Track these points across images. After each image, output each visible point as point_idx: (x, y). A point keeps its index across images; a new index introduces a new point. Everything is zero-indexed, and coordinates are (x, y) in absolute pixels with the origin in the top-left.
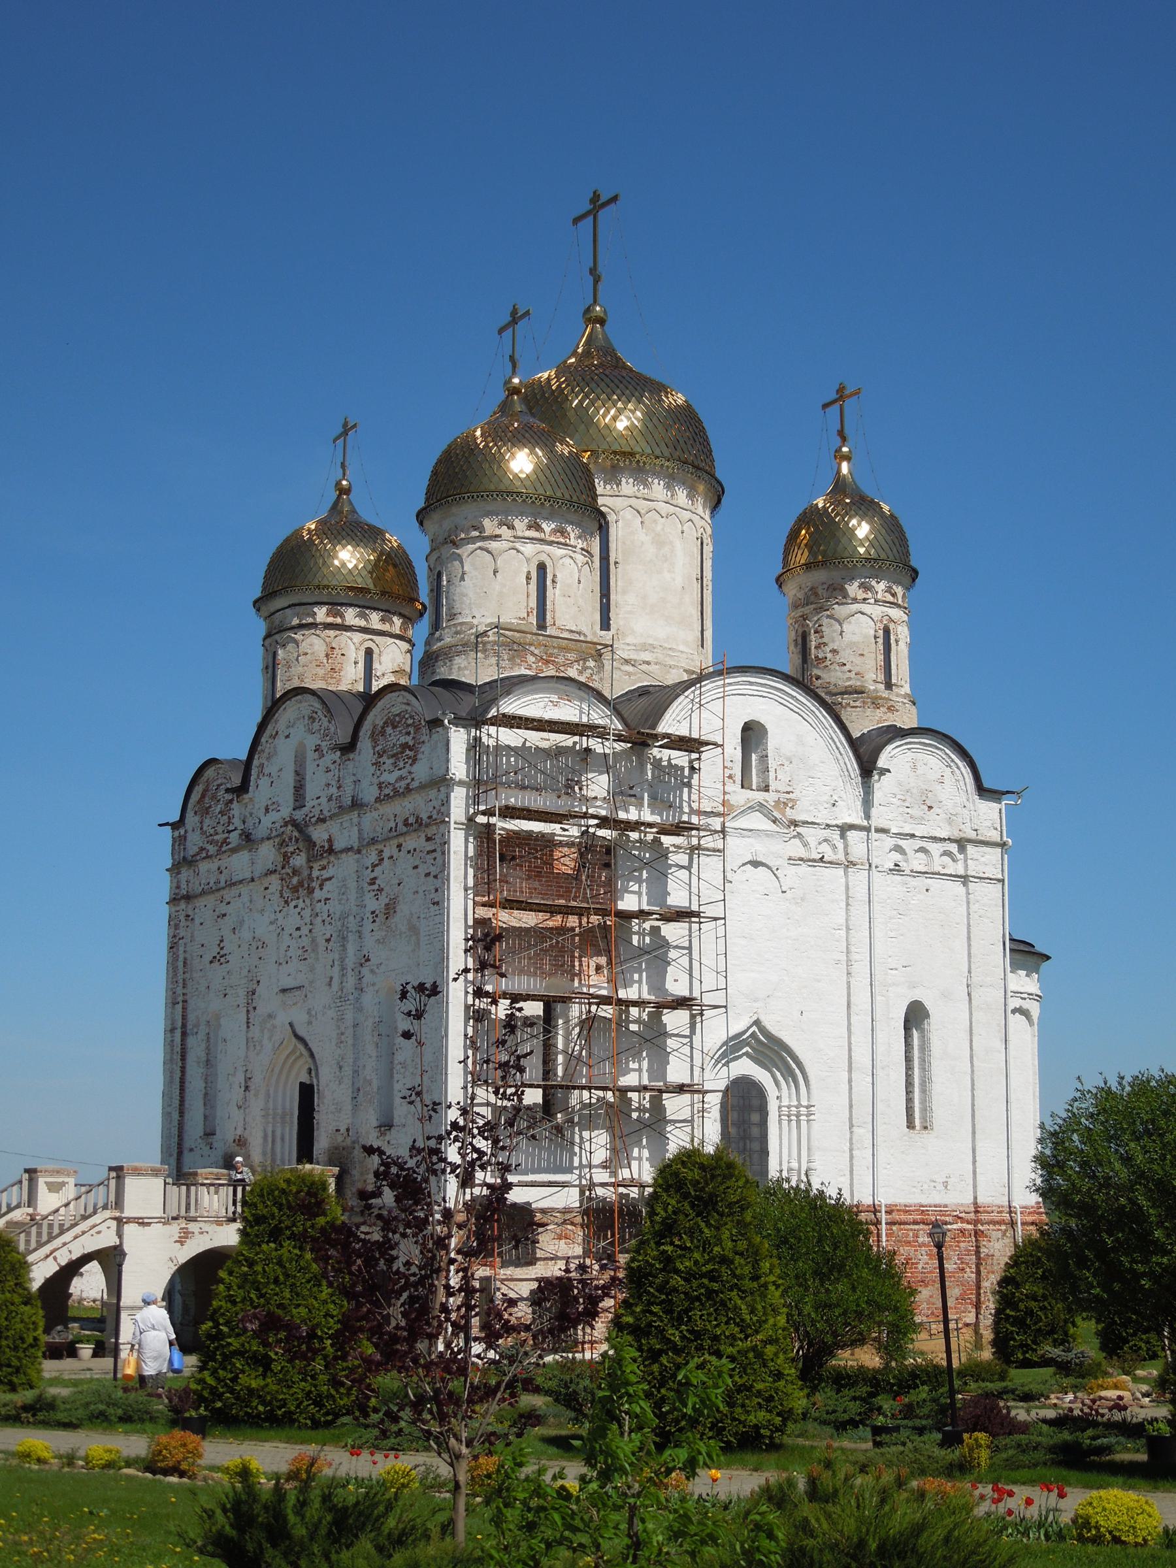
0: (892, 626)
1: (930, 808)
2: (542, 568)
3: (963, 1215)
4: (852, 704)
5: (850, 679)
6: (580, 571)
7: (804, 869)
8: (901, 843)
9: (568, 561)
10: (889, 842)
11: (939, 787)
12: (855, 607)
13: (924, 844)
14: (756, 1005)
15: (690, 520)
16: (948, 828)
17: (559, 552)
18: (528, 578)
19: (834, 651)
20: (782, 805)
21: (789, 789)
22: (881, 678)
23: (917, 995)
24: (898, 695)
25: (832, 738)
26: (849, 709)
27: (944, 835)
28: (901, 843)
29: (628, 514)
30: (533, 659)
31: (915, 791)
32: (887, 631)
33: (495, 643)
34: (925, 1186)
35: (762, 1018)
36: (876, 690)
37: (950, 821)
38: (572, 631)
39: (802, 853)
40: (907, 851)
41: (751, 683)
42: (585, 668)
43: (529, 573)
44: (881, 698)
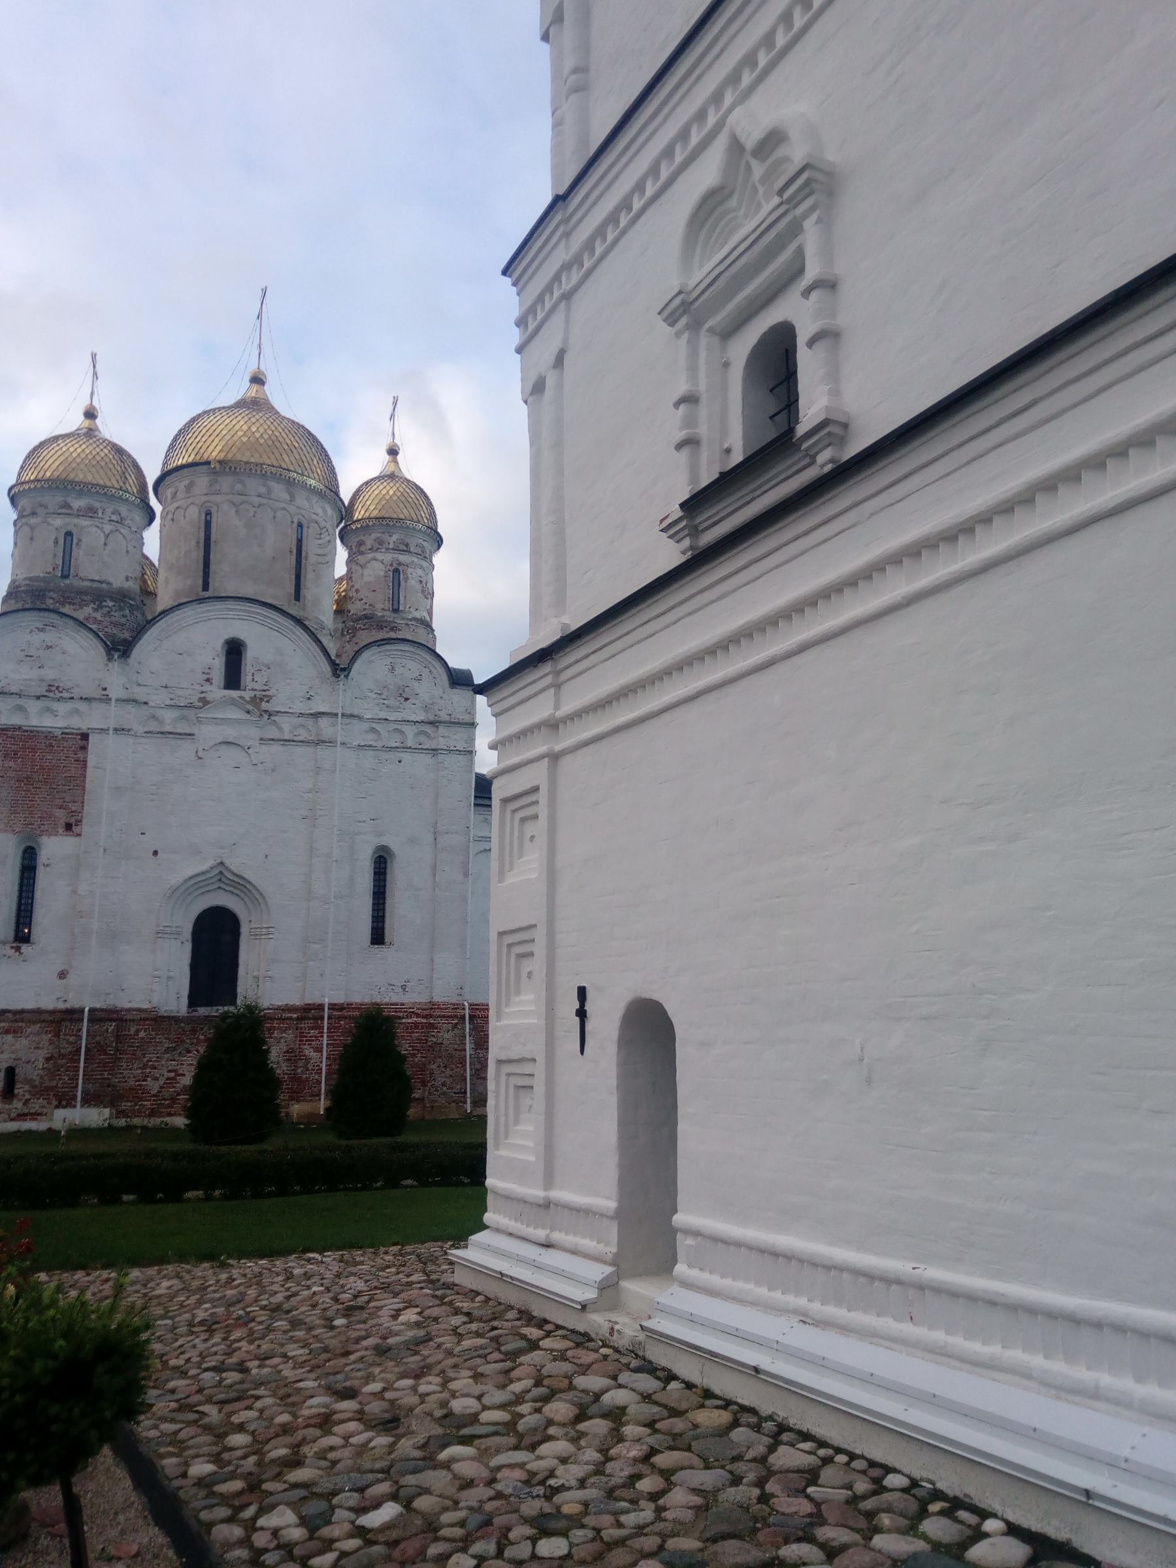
0: (401, 568)
1: (406, 699)
2: (69, 534)
3: (419, 1011)
4: (363, 627)
5: (365, 609)
6: (107, 536)
7: (276, 748)
8: (378, 727)
9: (94, 529)
10: (366, 726)
11: (416, 684)
12: (370, 556)
13: (399, 727)
14: (222, 851)
15: (284, 509)
16: (424, 714)
17: (84, 522)
18: (56, 542)
19: (357, 591)
20: (256, 701)
21: (266, 688)
22: (388, 605)
23: (384, 841)
24: (403, 619)
25: (309, 649)
26: (361, 631)
27: (418, 719)
28: (374, 725)
29: (225, 507)
30: (51, 601)
31: (391, 687)
32: (396, 571)
33: (23, 592)
34: (383, 989)
35: (227, 861)
36: (383, 616)
37: (426, 708)
38: (93, 581)
39: (275, 734)
40: (381, 732)
41: (232, 610)
42: (100, 607)
43: (56, 538)
44: (386, 621)
